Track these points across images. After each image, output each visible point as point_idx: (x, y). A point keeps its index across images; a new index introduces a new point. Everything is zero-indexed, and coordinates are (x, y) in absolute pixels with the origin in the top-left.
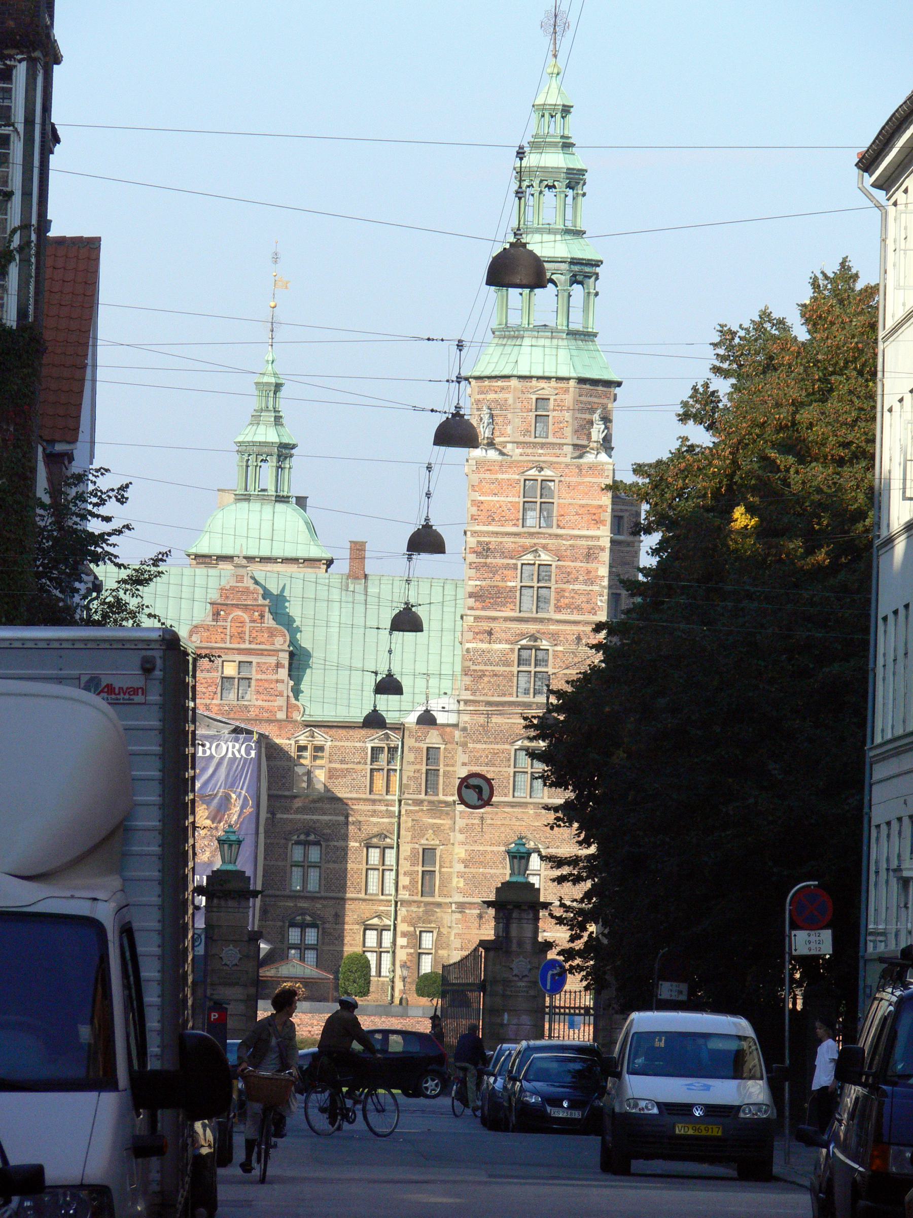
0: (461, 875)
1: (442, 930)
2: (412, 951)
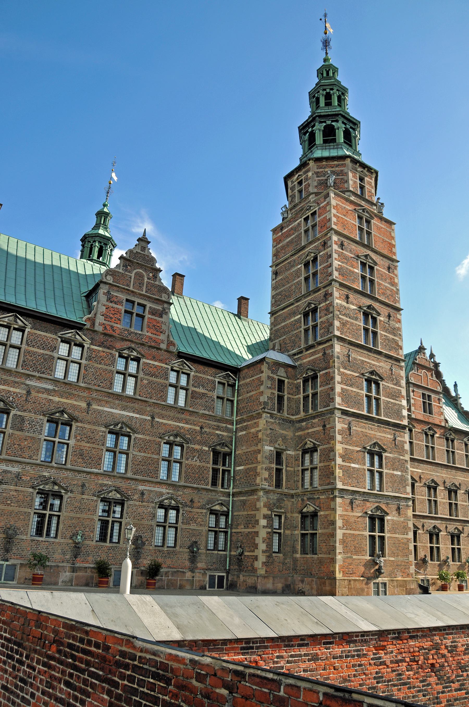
0: (341, 467)
2: (270, 530)
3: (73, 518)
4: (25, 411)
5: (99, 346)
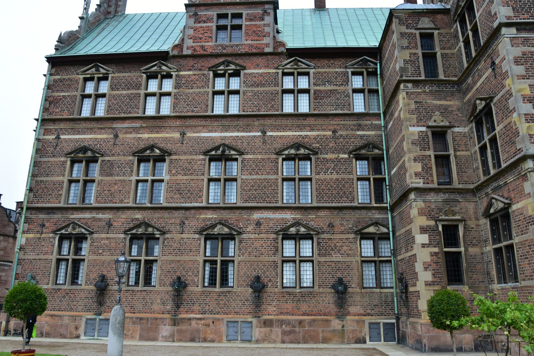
1: (469, 223)
2: (436, 250)
3: (173, 261)
4: (113, 155)
5: (190, 70)
